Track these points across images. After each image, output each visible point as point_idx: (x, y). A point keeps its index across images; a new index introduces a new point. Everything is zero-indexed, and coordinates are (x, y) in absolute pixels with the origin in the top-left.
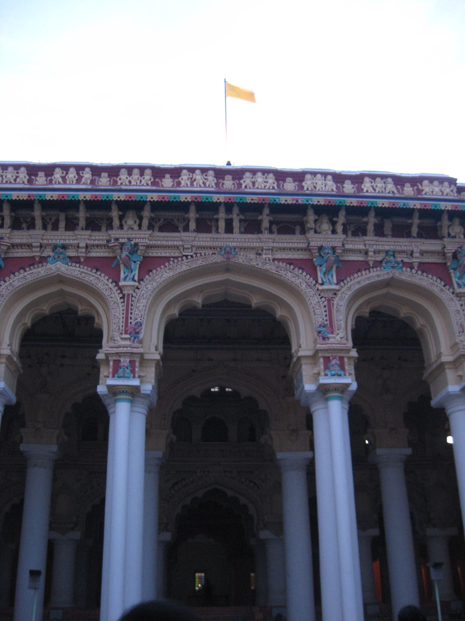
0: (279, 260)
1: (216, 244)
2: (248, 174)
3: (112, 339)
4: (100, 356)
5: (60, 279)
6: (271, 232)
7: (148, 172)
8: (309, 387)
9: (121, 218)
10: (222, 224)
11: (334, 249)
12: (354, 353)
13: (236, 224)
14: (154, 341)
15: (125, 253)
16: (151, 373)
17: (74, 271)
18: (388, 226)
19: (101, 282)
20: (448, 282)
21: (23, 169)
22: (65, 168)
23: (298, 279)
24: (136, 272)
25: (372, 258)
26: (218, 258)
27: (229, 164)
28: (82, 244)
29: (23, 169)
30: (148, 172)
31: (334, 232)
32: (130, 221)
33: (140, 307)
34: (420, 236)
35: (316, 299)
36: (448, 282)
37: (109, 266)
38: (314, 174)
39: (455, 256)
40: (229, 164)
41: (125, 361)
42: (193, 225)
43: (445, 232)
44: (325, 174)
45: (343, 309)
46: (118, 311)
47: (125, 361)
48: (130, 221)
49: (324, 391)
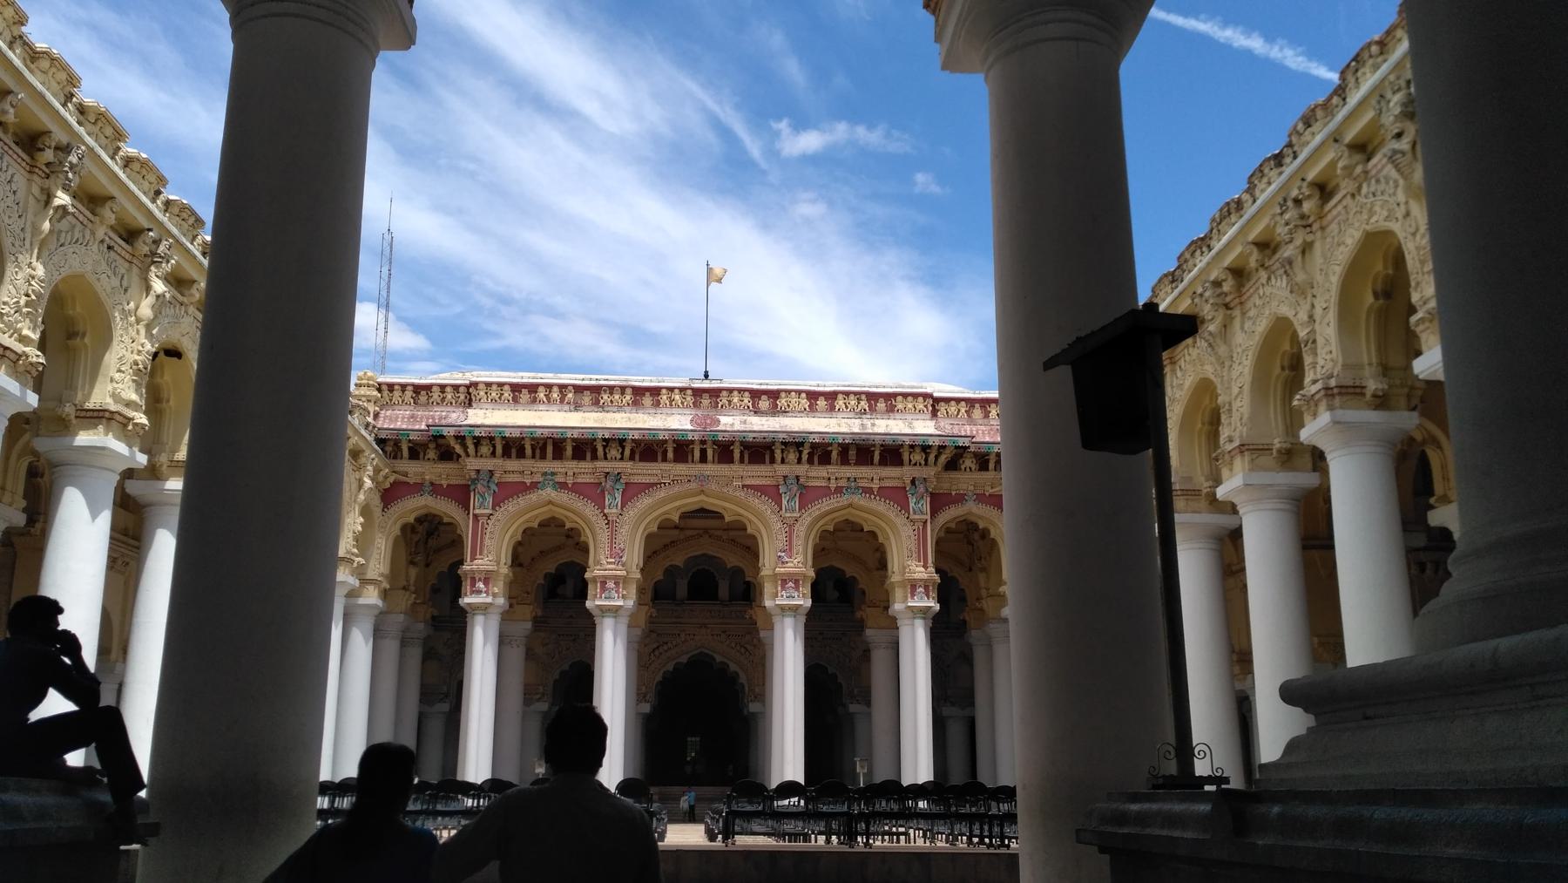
0: (748, 487)
1: (692, 473)
2: (724, 393)
3: (598, 563)
4: (587, 575)
5: (550, 502)
6: (742, 461)
7: (629, 391)
8: (768, 603)
9: (604, 447)
10: (697, 454)
11: (797, 478)
12: (812, 574)
13: (710, 456)
14: (636, 560)
15: (609, 483)
16: (633, 590)
17: (564, 497)
18: (852, 453)
19: (589, 510)
20: (904, 506)
21: (507, 388)
22: (549, 387)
23: (763, 505)
24: (619, 499)
25: (833, 485)
26: (693, 485)
27: (706, 376)
28: (570, 473)
29: (507, 388)
30: (629, 391)
31: (799, 461)
32: (614, 452)
33: (624, 531)
34: (884, 462)
35: (779, 525)
36: (904, 506)
37: (594, 493)
38: (789, 392)
39: (913, 482)
40: (706, 376)
41: (611, 584)
42: (670, 455)
43: (906, 457)
44: (799, 392)
45: (802, 534)
46: (603, 536)
47: (611, 584)
48: (614, 452)
49: (783, 608)
